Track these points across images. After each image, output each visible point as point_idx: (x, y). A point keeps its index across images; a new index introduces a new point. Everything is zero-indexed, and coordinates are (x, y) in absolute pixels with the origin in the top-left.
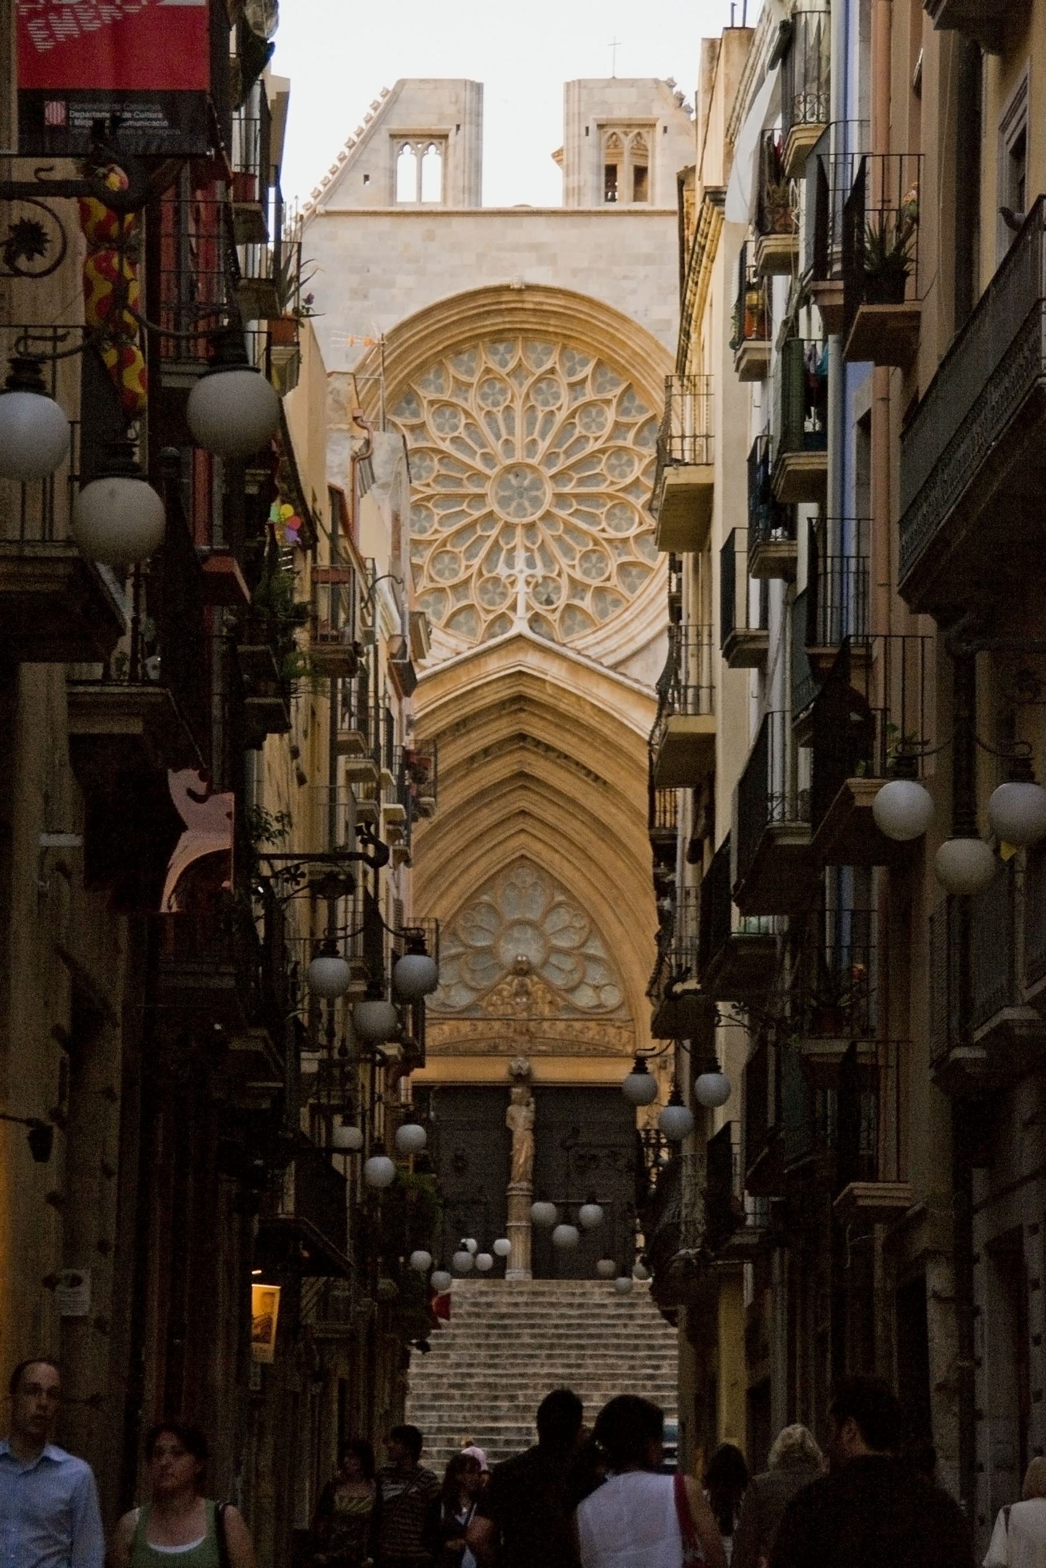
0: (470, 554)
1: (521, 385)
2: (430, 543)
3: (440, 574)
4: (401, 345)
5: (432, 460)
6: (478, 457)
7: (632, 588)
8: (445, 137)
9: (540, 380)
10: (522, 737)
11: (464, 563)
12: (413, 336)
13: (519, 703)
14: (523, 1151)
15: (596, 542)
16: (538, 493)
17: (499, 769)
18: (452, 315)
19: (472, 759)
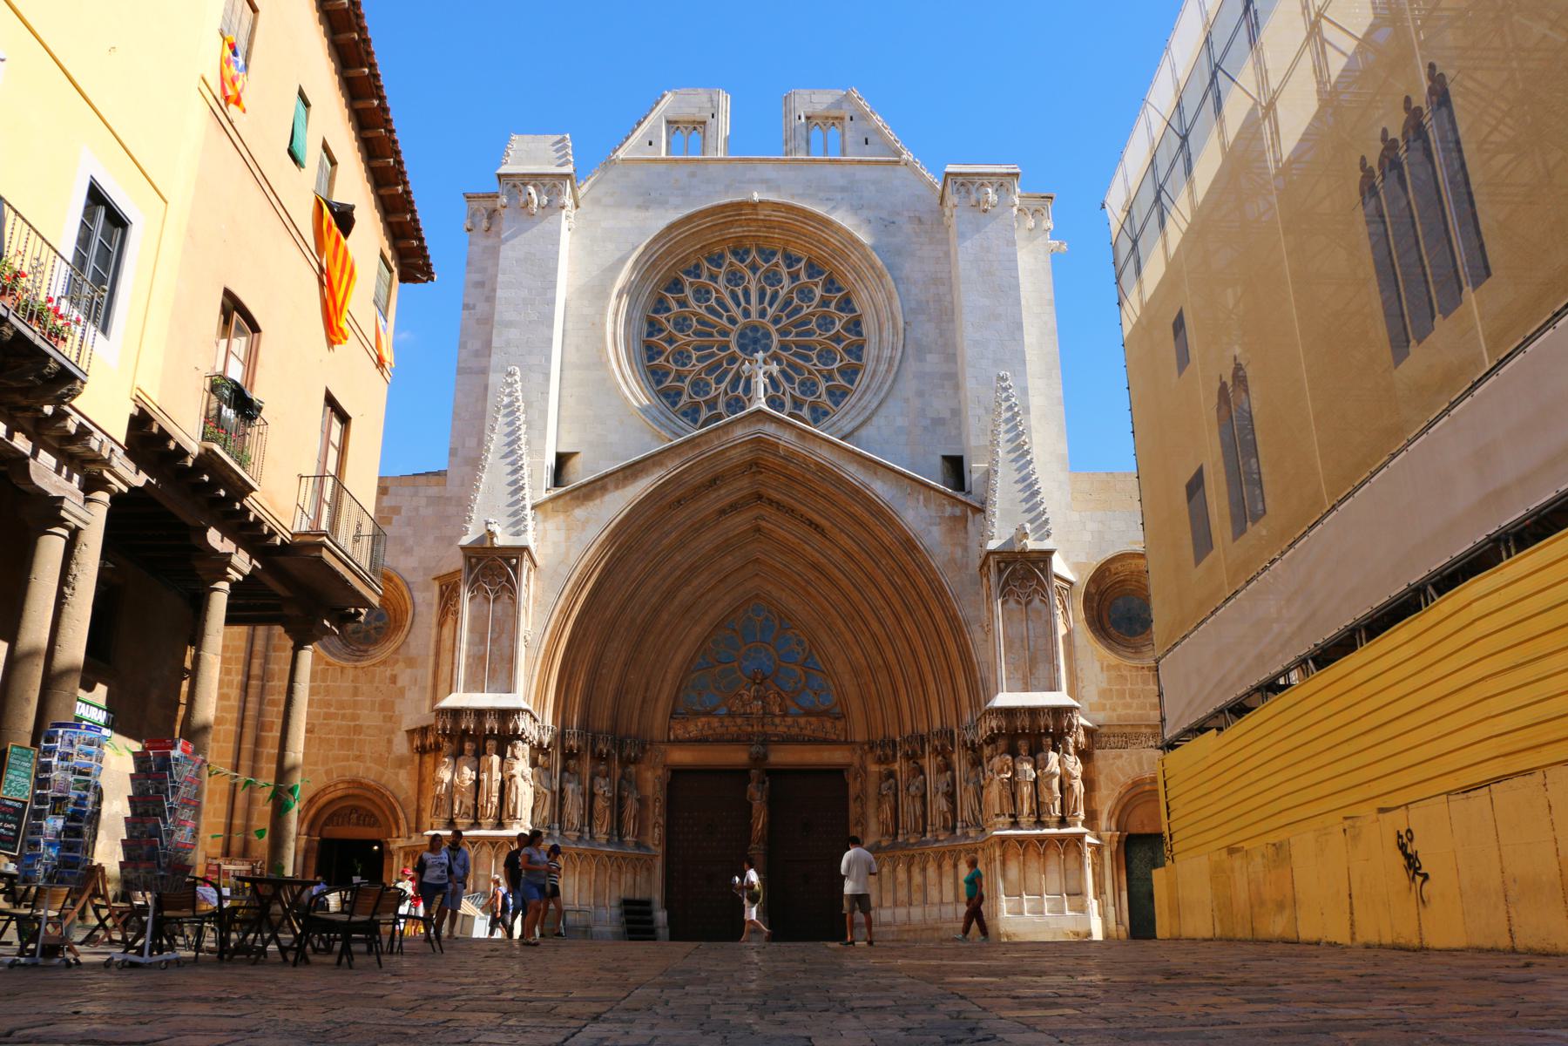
0: (719, 381)
1: (755, 274)
2: (690, 372)
3: (697, 393)
4: (670, 240)
5: (691, 320)
6: (724, 318)
7: (837, 404)
8: (704, 123)
9: (767, 270)
10: (760, 497)
11: (714, 386)
12: (680, 234)
13: (754, 466)
14: (760, 822)
15: (810, 373)
16: (768, 342)
17: (739, 522)
18: (708, 222)
19: (722, 512)
